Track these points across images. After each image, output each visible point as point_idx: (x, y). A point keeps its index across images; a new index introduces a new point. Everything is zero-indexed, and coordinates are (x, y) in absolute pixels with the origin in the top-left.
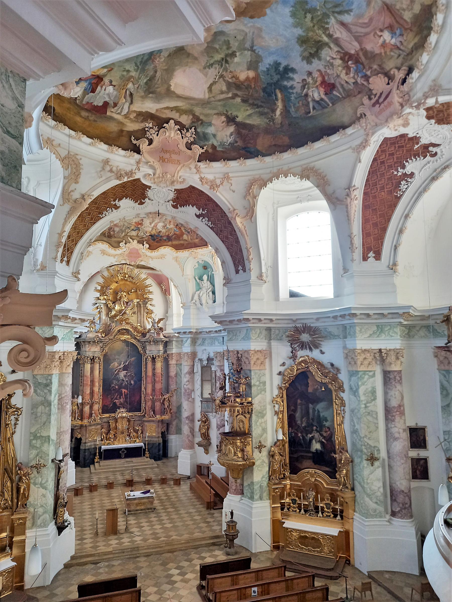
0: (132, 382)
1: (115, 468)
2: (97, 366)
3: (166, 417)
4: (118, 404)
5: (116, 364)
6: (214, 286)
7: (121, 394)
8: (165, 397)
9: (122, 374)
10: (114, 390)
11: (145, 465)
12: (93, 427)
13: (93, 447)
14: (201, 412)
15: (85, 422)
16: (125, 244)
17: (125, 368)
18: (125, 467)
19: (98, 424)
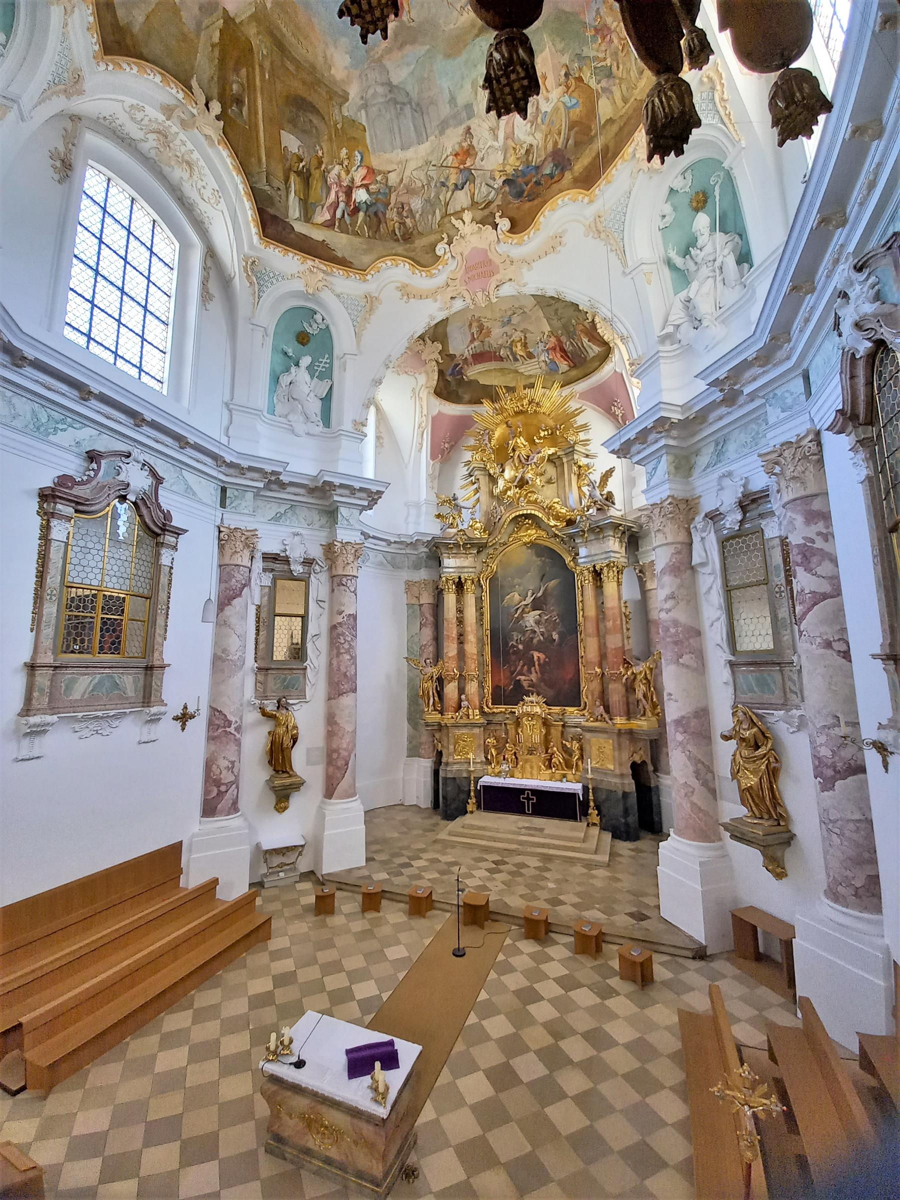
0: (555, 636)
1: (495, 840)
2: (470, 600)
3: (642, 724)
4: (525, 684)
5: (517, 597)
6: (742, 234)
7: (531, 662)
8: (636, 670)
9: (531, 618)
10: (515, 653)
11: (573, 849)
12: (464, 731)
13: (465, 775)
14: (735, 706)
15: (449, 718)
16: (449, 243)
17: (537, 605)
18: (521, 843)
19: (474, 725)
